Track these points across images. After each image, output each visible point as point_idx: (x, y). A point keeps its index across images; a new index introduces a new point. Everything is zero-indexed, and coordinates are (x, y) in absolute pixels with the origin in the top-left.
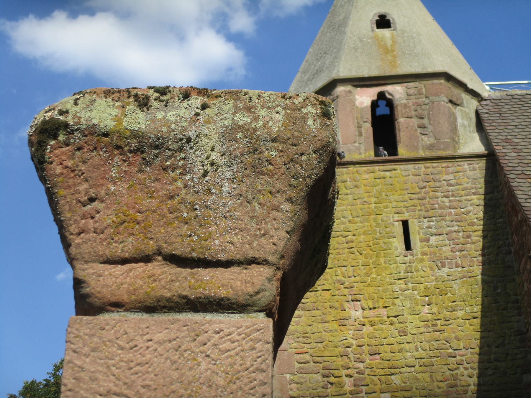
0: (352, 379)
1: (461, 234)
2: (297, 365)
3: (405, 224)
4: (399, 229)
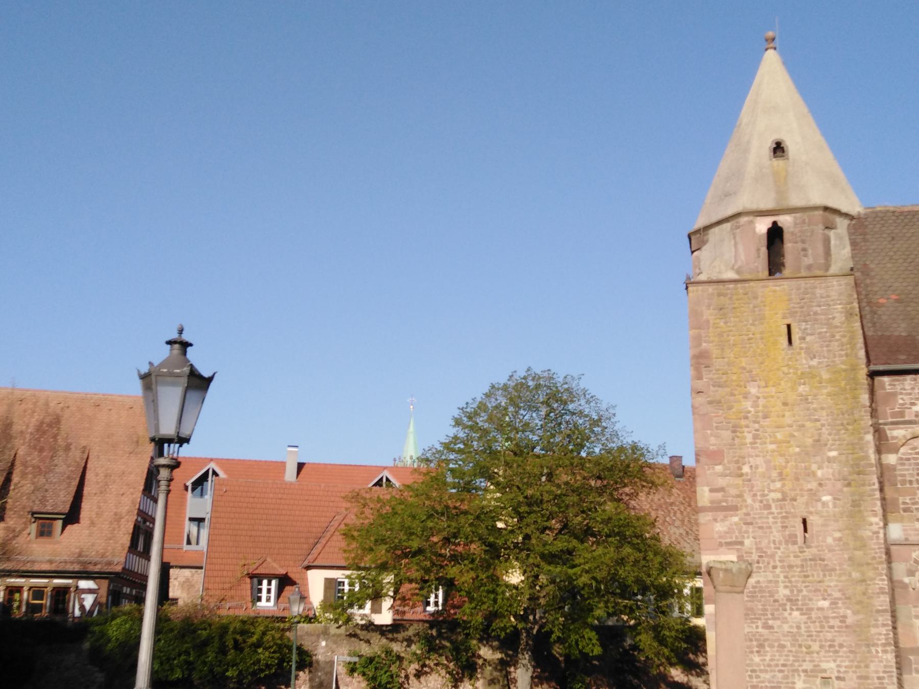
0: (751, 435)
1: (828, 334)
2: (715, 425)
3: (789, 327)
4: (784, 330)
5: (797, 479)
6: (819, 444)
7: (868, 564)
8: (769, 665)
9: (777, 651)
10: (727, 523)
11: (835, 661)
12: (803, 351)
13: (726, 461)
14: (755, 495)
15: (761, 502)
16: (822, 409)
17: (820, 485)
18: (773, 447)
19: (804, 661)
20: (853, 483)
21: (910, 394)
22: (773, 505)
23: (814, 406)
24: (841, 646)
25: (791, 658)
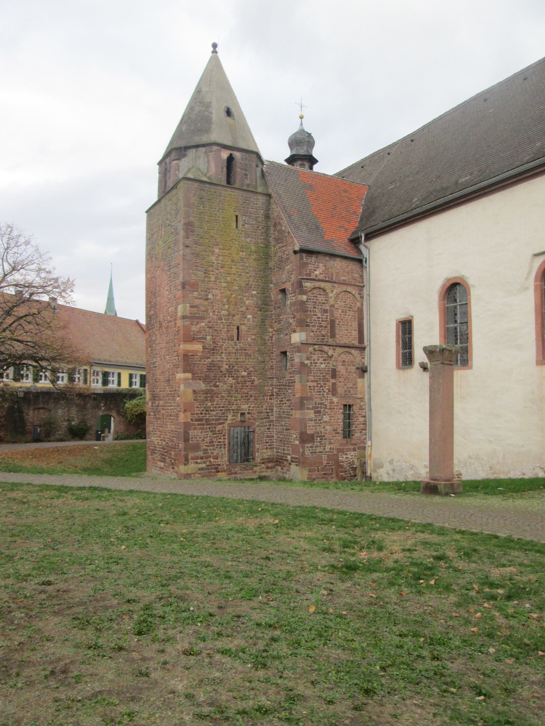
4: (235, 219)
5: (236, 304)
6: (248, 287)
7: (267, 353)
8: (216, 407)
9: (220, 399)
10: (198, 326)
11: (248, 404)
12: (243, 233)
13: (200, 289)
14: (214, 312)
15: (217, 315)
16: (250, 267)
17: (247, 309)
18: (225, 284)
19: (233, 404)
20: (262, 309)
21: (314, 265)
22: (223, 318)
23: (247, 264)
24: (251, 396)
25: (227, 403)
